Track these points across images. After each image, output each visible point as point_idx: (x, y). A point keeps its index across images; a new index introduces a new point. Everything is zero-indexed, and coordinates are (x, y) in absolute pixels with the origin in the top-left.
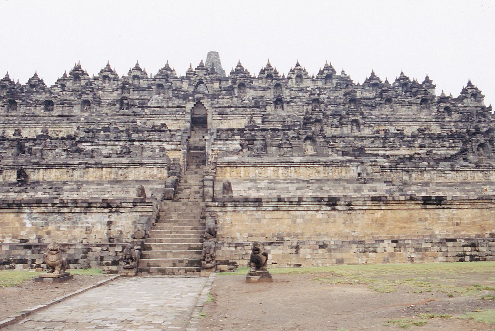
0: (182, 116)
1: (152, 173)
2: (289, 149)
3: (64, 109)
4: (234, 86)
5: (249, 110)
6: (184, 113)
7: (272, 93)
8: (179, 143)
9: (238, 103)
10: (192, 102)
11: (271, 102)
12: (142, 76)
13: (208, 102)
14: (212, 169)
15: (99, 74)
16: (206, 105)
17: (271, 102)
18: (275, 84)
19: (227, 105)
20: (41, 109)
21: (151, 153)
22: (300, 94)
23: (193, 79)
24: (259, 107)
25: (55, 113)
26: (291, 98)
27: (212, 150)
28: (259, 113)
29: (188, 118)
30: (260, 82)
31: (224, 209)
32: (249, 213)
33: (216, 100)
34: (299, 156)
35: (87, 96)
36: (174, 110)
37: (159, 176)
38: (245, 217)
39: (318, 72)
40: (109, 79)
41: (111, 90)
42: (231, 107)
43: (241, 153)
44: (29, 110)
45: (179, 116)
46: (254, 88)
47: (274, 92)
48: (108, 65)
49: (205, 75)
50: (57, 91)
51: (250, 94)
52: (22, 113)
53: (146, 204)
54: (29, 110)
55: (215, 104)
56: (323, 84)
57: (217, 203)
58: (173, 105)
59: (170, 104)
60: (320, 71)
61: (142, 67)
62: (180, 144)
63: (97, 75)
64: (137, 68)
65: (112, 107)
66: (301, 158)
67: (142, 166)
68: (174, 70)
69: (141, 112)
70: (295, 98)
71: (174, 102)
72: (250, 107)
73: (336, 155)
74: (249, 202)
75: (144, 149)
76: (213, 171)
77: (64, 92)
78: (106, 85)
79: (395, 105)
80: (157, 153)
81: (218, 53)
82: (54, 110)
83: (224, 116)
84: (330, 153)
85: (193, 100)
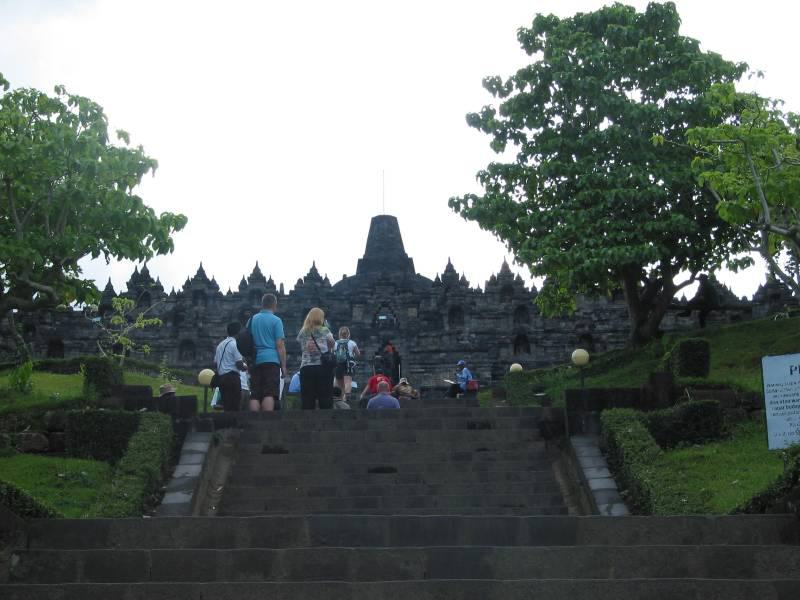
4: (443, 312)
5: (469, 356)
7: (511, 322)
11: (508, 341)
17: (508, 341)
19: (434, 348)
22: (563, 324)
23: (372, 302)
24: (486, 351)
26: (549, 331)
28: (486, 360)
30: (489, 300)
33: (415, 339)
35: (186, 333)
40: (206, 298)
42: (438, 351)
46: (479, 315)
47: (514, 321)
48: (201, 272)
49: (392, 294)
51: (471, 325)
55: (414, 347)
56: (609, 302)
61: (266, 273)
63: (179, 288)
64: (257, 275)
68: (326, 278)
70: (552, 331)
72: (471, 351)
78: (200, 308)
81: (395, 219)
85: (378, 342)
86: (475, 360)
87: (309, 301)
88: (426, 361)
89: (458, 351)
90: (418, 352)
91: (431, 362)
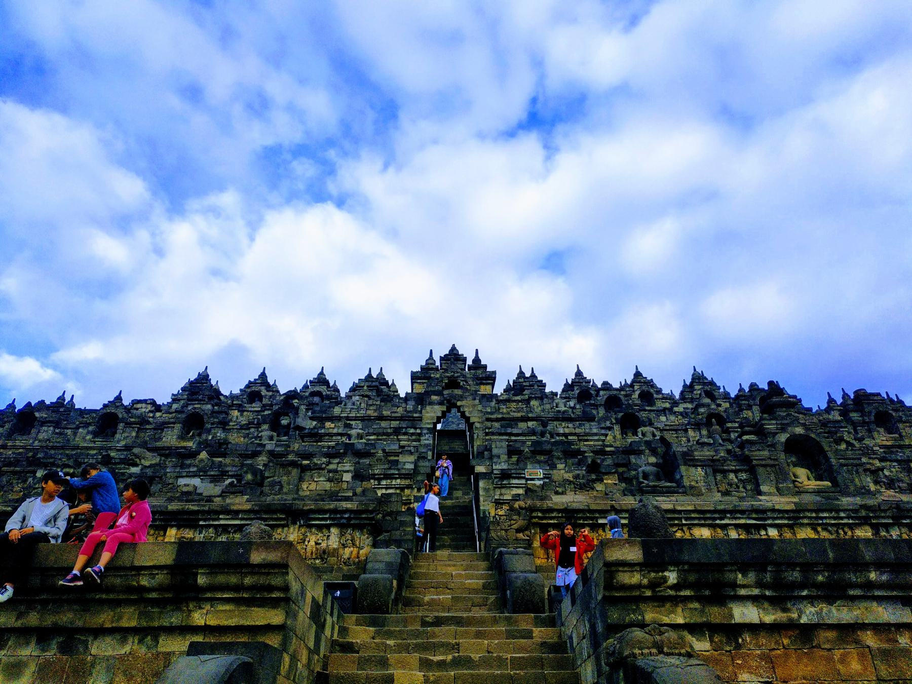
0: (414, 437)
1: (324, 545)
2: (744, 476)
3: (142, 435)
5: (570, 425)
6: (418, 431)
8: (407, 482)
9: (543, 410)
10: (436, 407)
12: (328, 393)
13: (474, 406)
14: (518, 531)
15: (241, 390)
16: (470, 412)
18: (606, 397)
19: (519, 415)
20: (88, 433)
21: (328, 486)
23: (438, 376)
25: (118, 442)
27: (498, 503)
28: (595, 431)
29: (427, 442)
31: (715, 614)
32: (870, 639)
34: (780, 492)
36: (395, 424)
37: (346, 556)
38: (855, 666)
39: (681, 389)
41: (259, 409)
43: (599, 487)
44: (60, 434)
45: (406, 437)
48: (263, 375)
50: (144, 410)
52: (40, 441)
53: (248, 581)
54: (60, 434)
57: (672, 577)
58: (393, 415)
59: (386, 413)
60: (685, 386)
62: (409, 487)
65: (252, 430)
66: (796, 500)
67: (294, 523)
68: (393, 384)
69: (315, 428)
71: (395, 409)
72: (570, 420)
73: (891, 492)
74: (863, 567)
75: (308, 473)
76: (520, 535)
77: (158, 414)
79: (901, 426)
80: (345, 486)
82: (117, 436)
83: (513, 438)
84: (873, 487)
85: (441, 403)
86: (578, 431)
87: (365, 388)
88: (509, 430)
89: (557, 419)
90: (497, 420)
91: (515, 431)
